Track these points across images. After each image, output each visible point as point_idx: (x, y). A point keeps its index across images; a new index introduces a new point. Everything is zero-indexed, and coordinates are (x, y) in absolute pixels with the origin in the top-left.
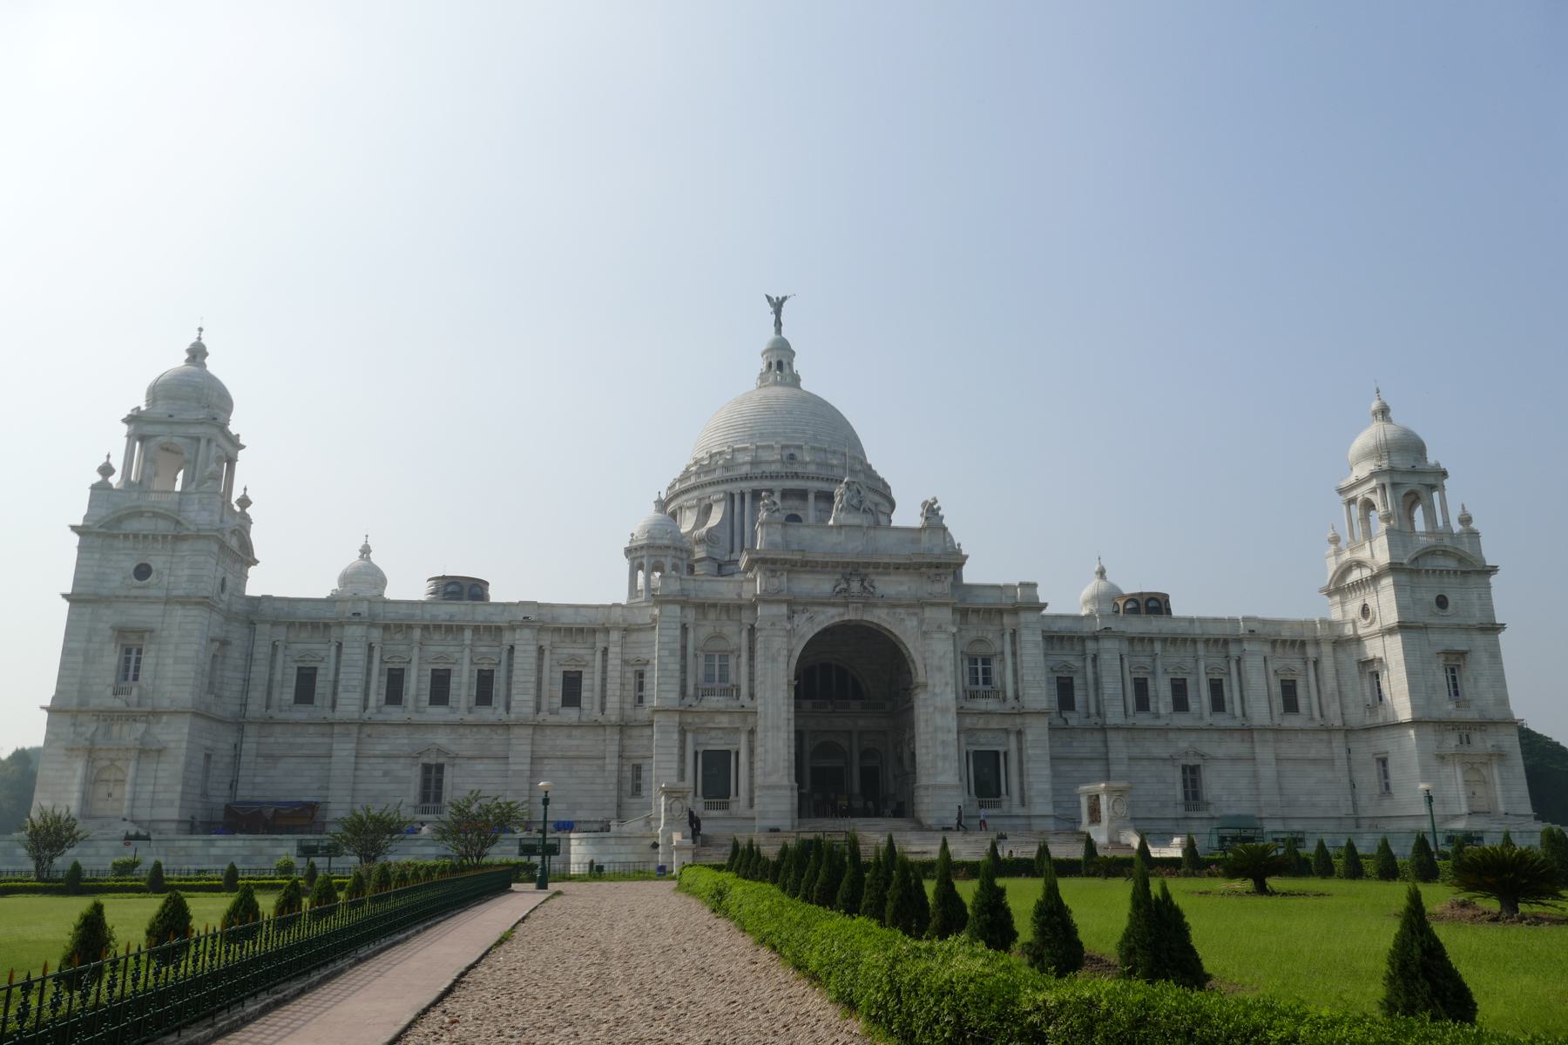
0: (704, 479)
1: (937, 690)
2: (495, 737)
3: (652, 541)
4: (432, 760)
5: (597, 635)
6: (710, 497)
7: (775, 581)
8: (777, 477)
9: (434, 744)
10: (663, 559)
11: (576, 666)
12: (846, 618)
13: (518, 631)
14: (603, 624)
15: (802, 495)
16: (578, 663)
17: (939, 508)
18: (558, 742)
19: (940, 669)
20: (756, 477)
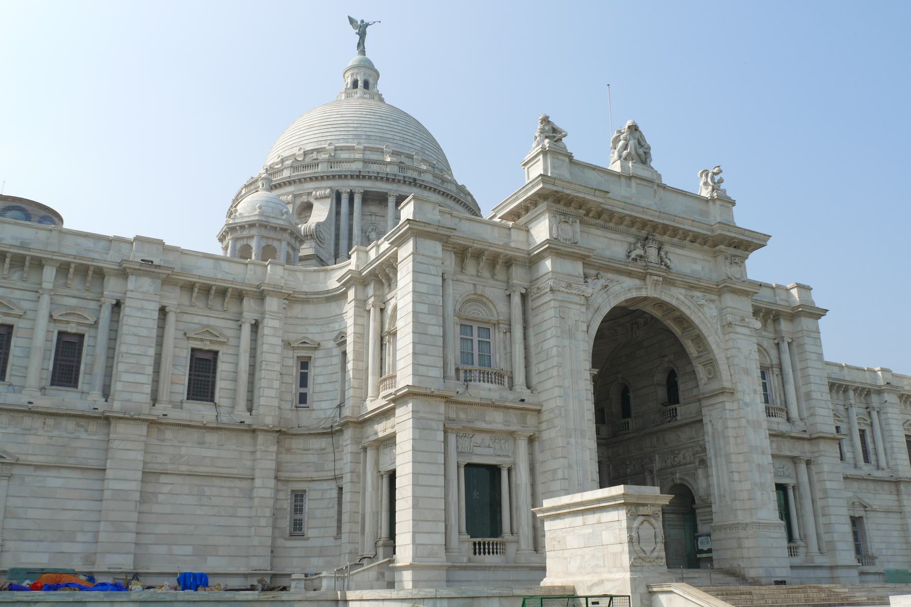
0: (308, 172)
1: (747, 399)
2: (84, 435)
3: (264, 219)
5: (245, 301)
6: (310, 194)
7: (567, 227)
8: (394, 180)
10: (275, 244)
11: (211, 341)
12: (644, 293)
13: (132, 279)
14: (258, 287)
16: (215, 339)
17: (721, 181)
18: (183, 451)
19: (747, 372)
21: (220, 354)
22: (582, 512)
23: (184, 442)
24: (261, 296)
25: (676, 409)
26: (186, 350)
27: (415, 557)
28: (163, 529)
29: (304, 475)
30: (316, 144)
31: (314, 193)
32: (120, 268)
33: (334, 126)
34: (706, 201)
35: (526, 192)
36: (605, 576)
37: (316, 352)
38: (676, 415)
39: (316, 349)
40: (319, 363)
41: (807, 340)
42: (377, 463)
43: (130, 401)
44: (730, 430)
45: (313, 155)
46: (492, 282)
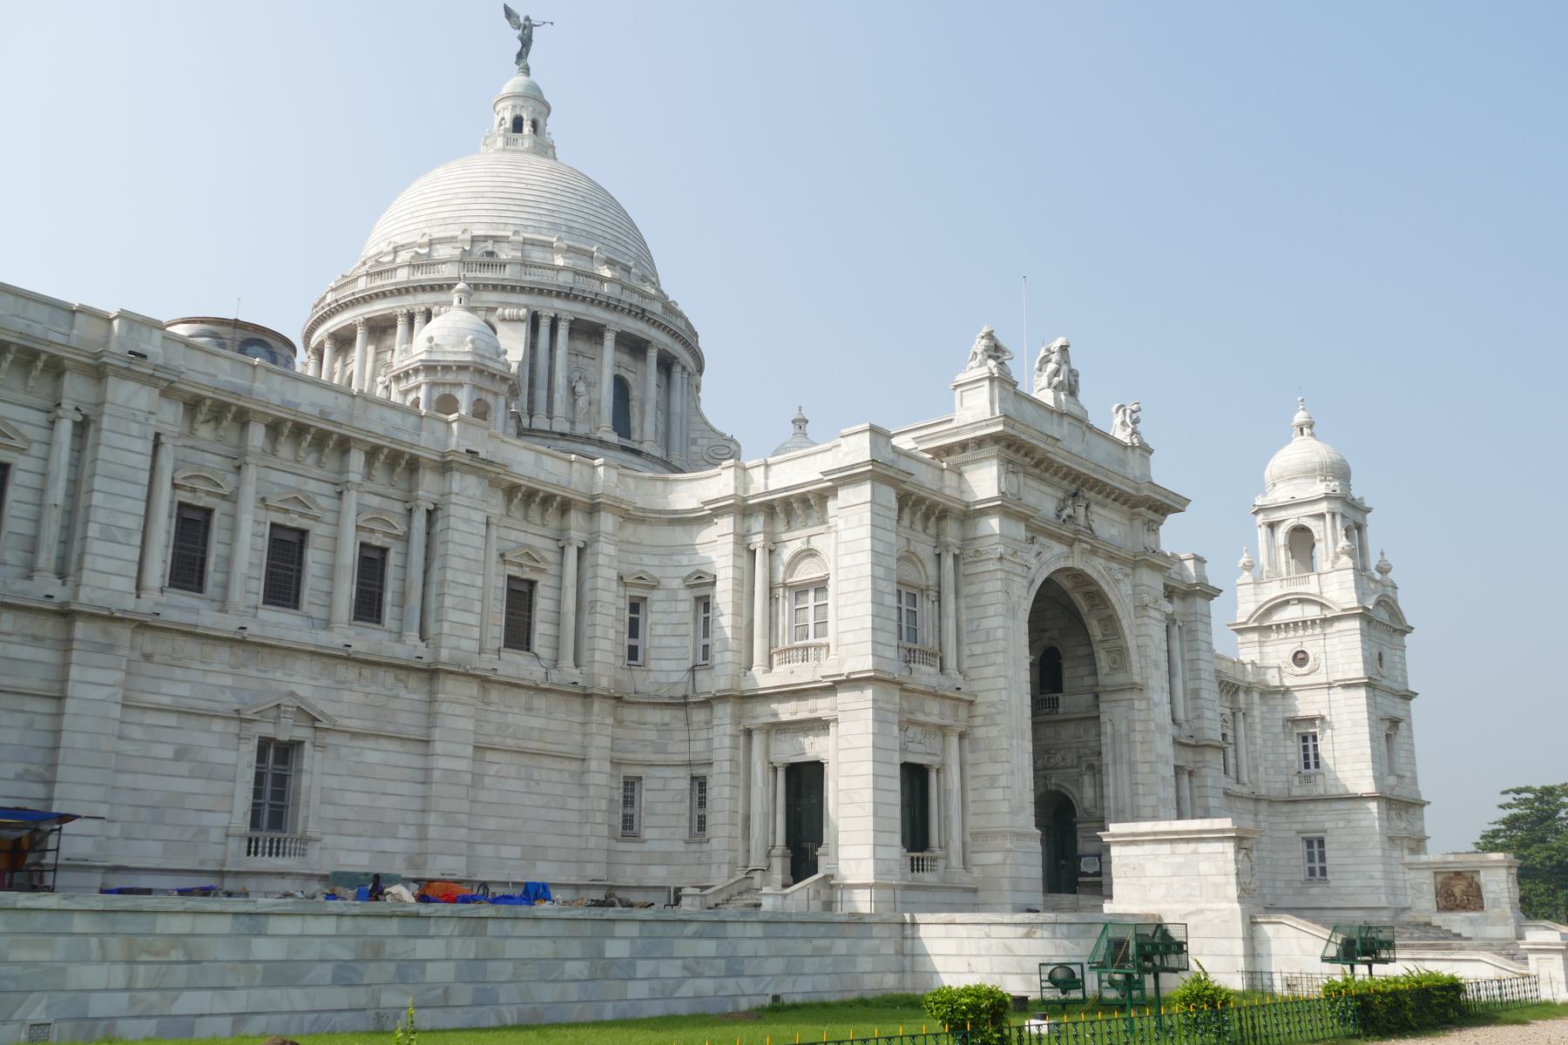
2: (403, 693)
4: (286, 732)
6: (494, 309)
9: (292, 694)
10: (489, 398)
12: (1070, 564)
15: (634, 346)
20: (584, 299)
21: (539, 585)
22: (1171, 841)
23: (510, 707)
24: (593, 508)
25: (1057, 699)
26: (502, 578)
27: (877, 873)
28: (491, 823)
29: (640, 757)
30: (484, 226)
31: (500, 310)
32: (443, 460)
33: (517, 202)
34: (1125, 447)
35: (974, 430)
36: (1203, 906)
37: (654, 592)
38: (1058, 706)
39: (653, 587)
40: (657, 607)
41: (1201, 626)
42: (767, 752)
43: (458, 648)
44: (1137, 733)
45: (486, 244)
46: (923, 537)
